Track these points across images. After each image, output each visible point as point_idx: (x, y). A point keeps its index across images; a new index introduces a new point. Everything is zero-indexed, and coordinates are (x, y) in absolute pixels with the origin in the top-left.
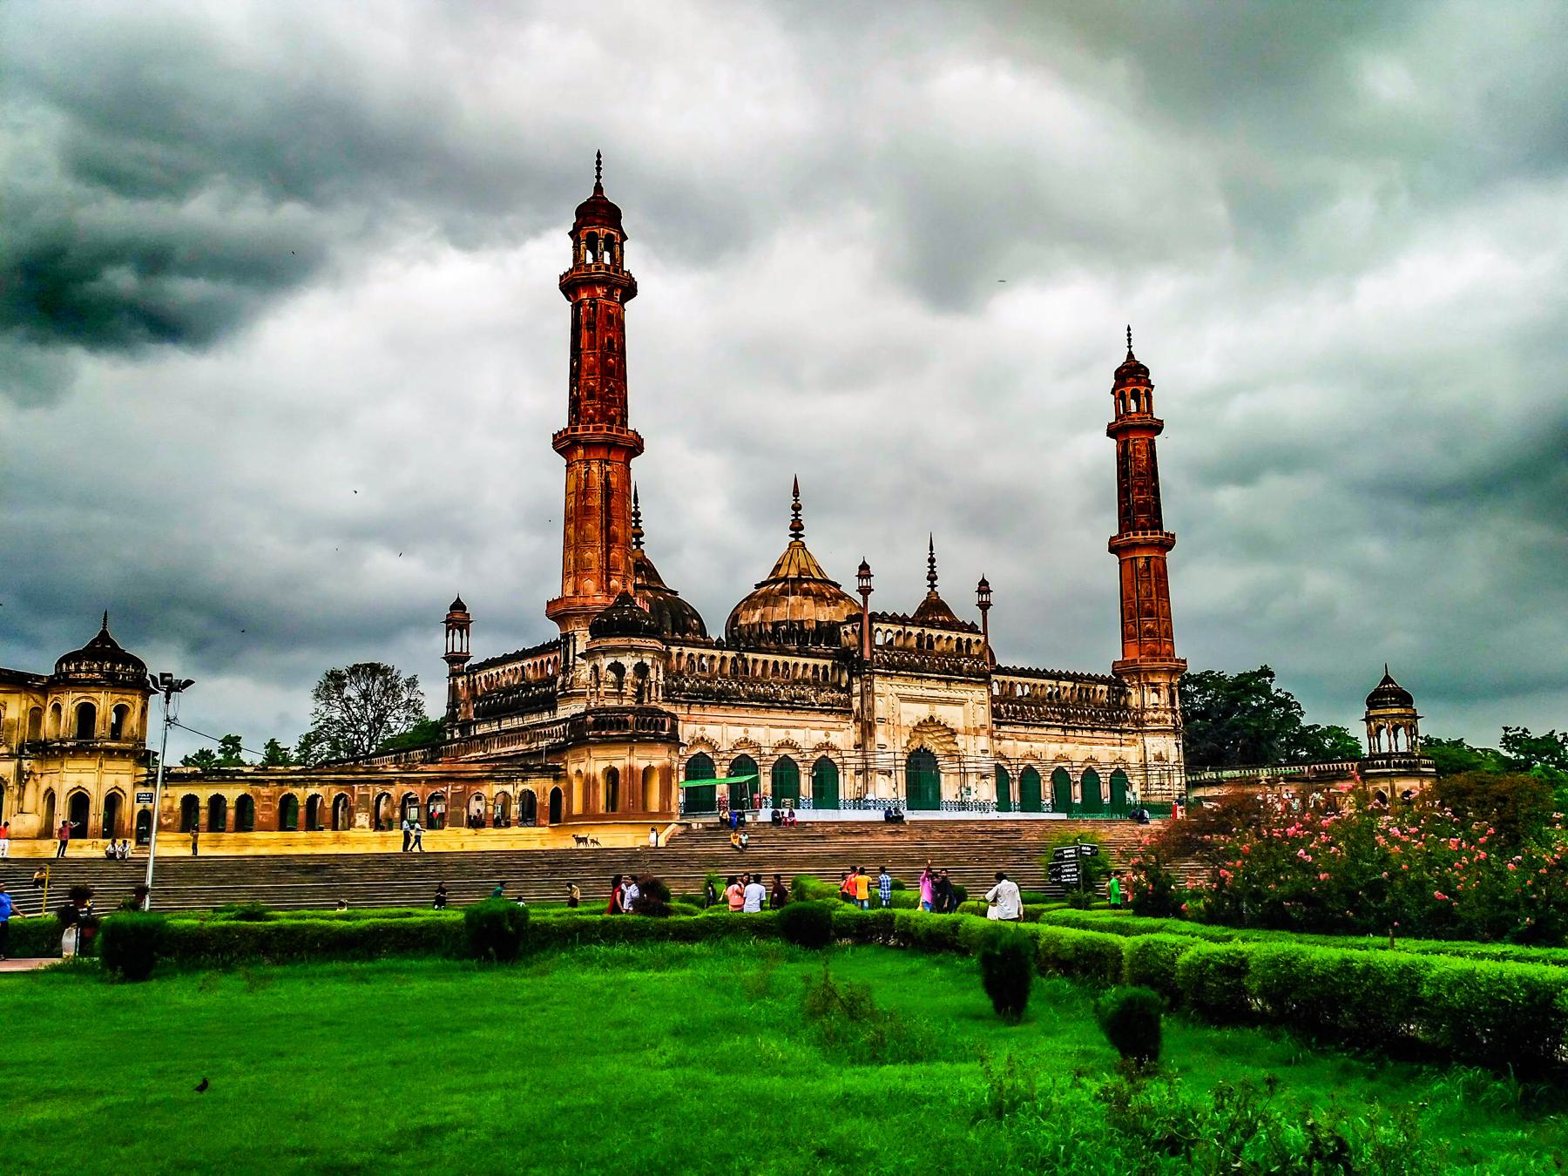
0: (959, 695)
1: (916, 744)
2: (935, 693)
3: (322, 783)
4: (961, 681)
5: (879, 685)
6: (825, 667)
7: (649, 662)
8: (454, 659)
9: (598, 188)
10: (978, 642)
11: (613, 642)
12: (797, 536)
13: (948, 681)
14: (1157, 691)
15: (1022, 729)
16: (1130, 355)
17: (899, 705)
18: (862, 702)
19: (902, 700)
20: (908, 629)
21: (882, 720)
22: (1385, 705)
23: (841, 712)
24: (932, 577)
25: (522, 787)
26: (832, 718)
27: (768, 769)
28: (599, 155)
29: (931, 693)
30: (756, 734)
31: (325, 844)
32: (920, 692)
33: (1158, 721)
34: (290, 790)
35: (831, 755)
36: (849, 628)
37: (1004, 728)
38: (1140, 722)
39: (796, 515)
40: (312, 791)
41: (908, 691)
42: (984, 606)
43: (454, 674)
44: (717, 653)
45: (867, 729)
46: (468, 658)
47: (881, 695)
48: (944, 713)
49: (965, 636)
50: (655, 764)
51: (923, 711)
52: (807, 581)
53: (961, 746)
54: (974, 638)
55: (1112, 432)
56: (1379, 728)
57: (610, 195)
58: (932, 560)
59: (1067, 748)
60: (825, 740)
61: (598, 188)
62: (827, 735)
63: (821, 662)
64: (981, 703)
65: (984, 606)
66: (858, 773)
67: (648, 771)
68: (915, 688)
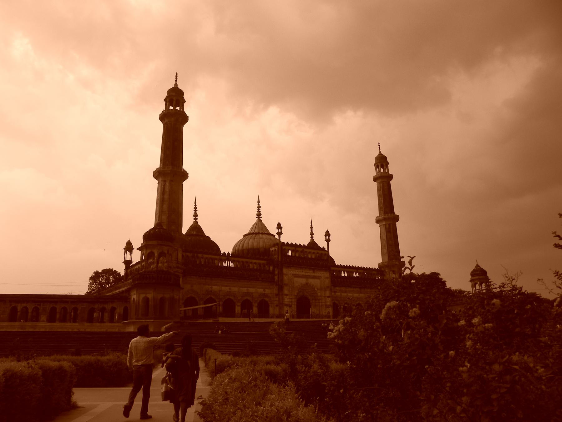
0: (318, 275)
2: (309, 274)
5: (285, 271)
7: (166, 252)
8: (127, 263)
9: (176, 84)
10: (325, 254)
11: (151, 243)
14: (394, 273)
15: (343, 289)
16: (380, 152)
17: (295, 278)
18: (278, 278)
20: (297, 249)
21: (286, 284)
24: (312, 234)
27: (239, 304)
28: (177, 74)
30: (235, 289)
31: (29, 327)
32: (302, 273)
34: (14, 305)
35: (267, 299)
36: (273, 249)
37: (337, 288)
39: (259, 210)
40: (24, 305)
41: (297, 273)
42: (328, 241)
43: (126, 269)
44: (218, 257)
45: (281, 288)
46: (131, 262)
47: (286, 275)
48: (311, 281)
49: (320, 252)
50: (167, 296)
51: (303, 281)
52: (262, 234)
53: (319, 294)
54: (323, 252)
55: (375, 180)
56: (476, 284)
57: (179, 87)
58: (312, 228)
59: (362, 295)
61: (176, 84)
62: (264, 291)
63: (262, 262)
64: (327, 278)
65: (328, 241)
66: (277, 306)
67: (162, 300)
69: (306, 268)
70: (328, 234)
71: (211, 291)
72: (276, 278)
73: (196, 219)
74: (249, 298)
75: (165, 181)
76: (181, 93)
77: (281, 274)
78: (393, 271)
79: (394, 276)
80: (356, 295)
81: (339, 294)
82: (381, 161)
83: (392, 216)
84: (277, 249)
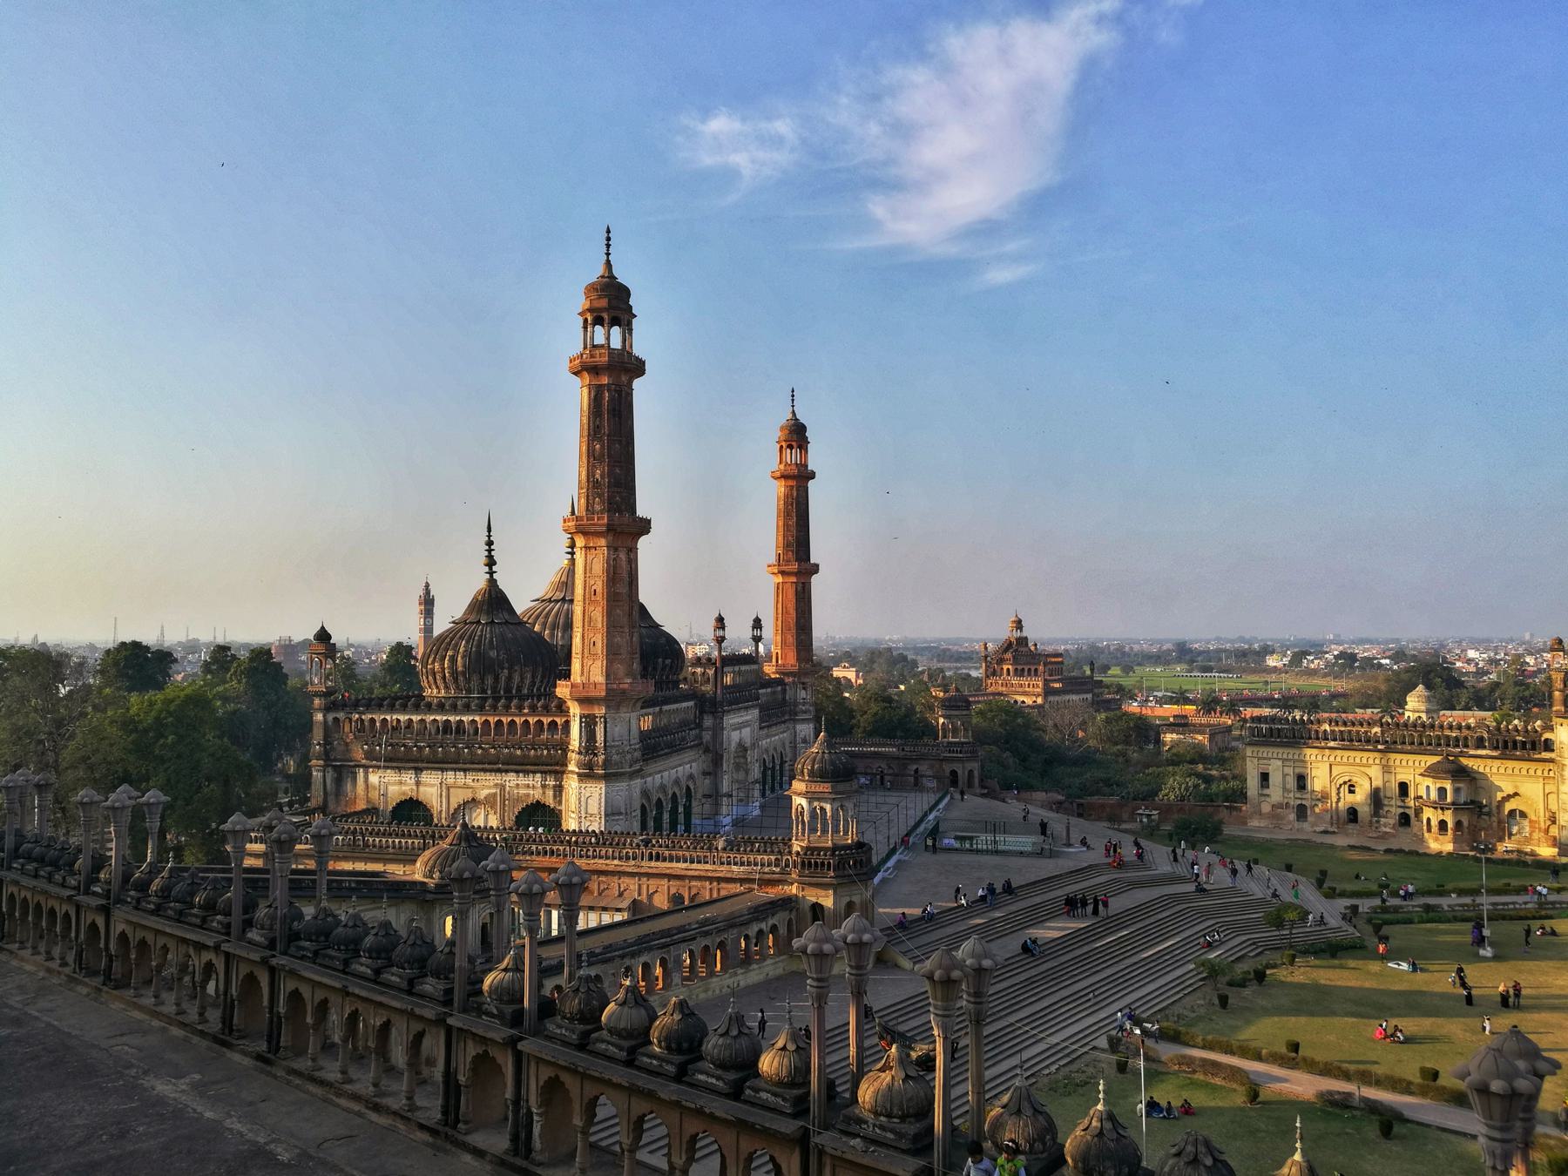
3: (650, 949)
9: (608, 264)
11: (841, 787)
22: (958, 708)
25: (771, 922)
28: (608, 231)
45: (717, 761)
54: (754, 667)
57: (622, 276)
61: (608, 264)
63: (691, 703)
72: (707, 736)
73: (491, 573)
75: (616, 549)
76: (624, 292)
77: (718, 729)
79: (803, 694)
82: (797, 435)
84: (711, 672)
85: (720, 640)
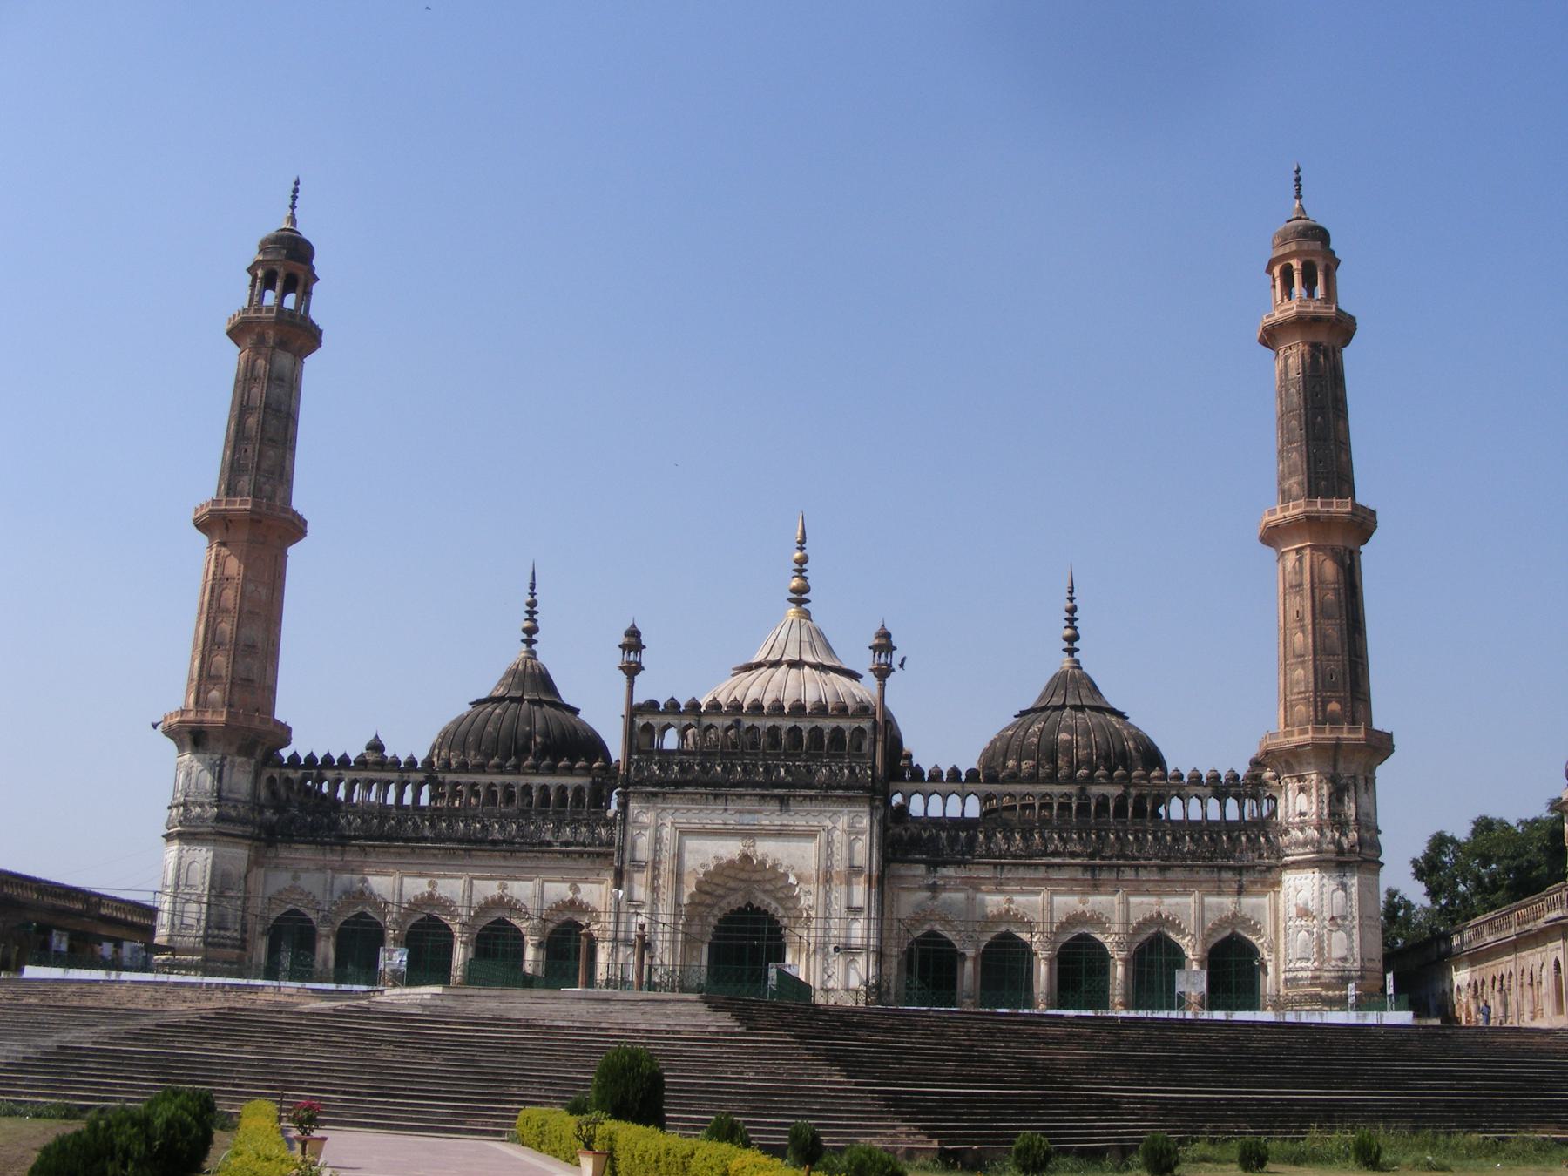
1: (736, 901)
4: (811, 798)
6: (579, 790)
12: (799, 602)
13: (783, 801)
14: (1302, 790)
15: (986, 873)
19: (684, 832)
21: (639, 866)
23: (599, 855)
26: (584, 863)
28: (297, 183)
29: (747, 818)
33: (1305, 844)
38: (1277, 852)
42: (883, 673)
48: (767, 849)
51: (731, 849)
58: (1072, 610)
59: (1100, 902)
60: (570, 895)
63: (571, 781)
65: (883, 673)
68: (714, 816)
69: (740, 796)
70: (884, 644)
71: (362, 893)
73: (529, 642)
74: (506, 915)
78: (1300, 779)
80: (1068, 903)
81: (961, 896)
83: (1339, 507)
85: (632, 670)
